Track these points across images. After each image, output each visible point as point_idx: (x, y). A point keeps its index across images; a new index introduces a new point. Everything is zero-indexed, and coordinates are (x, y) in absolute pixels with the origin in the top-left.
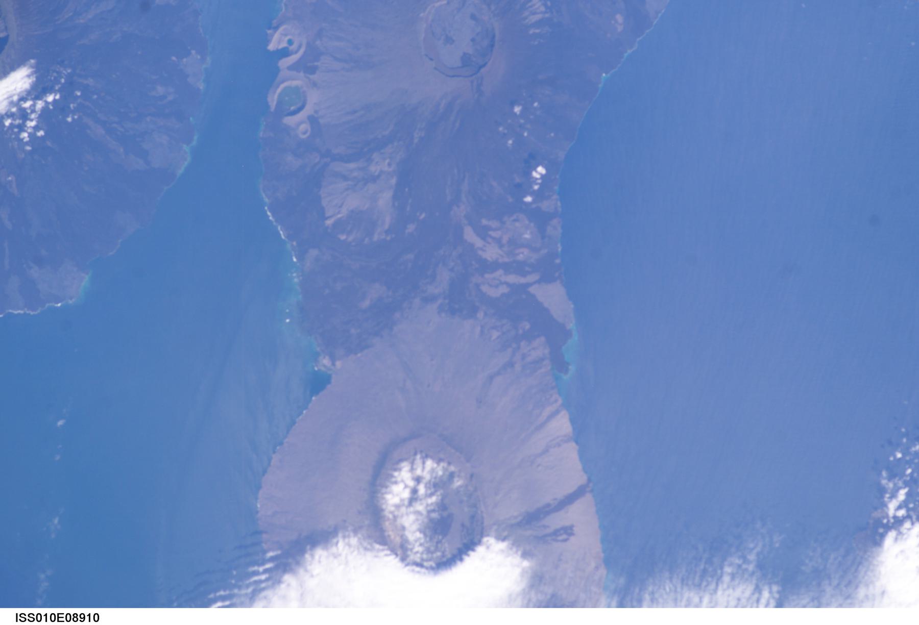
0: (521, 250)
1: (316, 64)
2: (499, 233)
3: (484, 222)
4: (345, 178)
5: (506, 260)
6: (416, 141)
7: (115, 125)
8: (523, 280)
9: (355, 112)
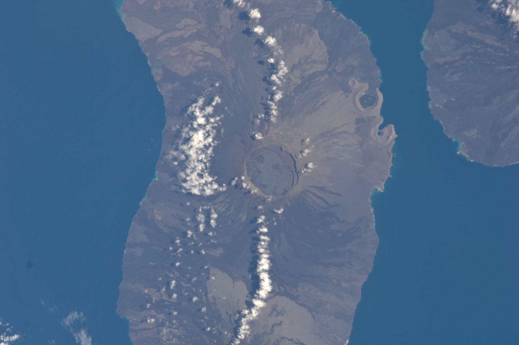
0: (176, 54)
1: (358, 126)
2: (196, 60)
3: (209, 63)
4: (314, 62)
5: (185, 44)
7: (479, 47)
8: (168, 35)
9: (323, 104)
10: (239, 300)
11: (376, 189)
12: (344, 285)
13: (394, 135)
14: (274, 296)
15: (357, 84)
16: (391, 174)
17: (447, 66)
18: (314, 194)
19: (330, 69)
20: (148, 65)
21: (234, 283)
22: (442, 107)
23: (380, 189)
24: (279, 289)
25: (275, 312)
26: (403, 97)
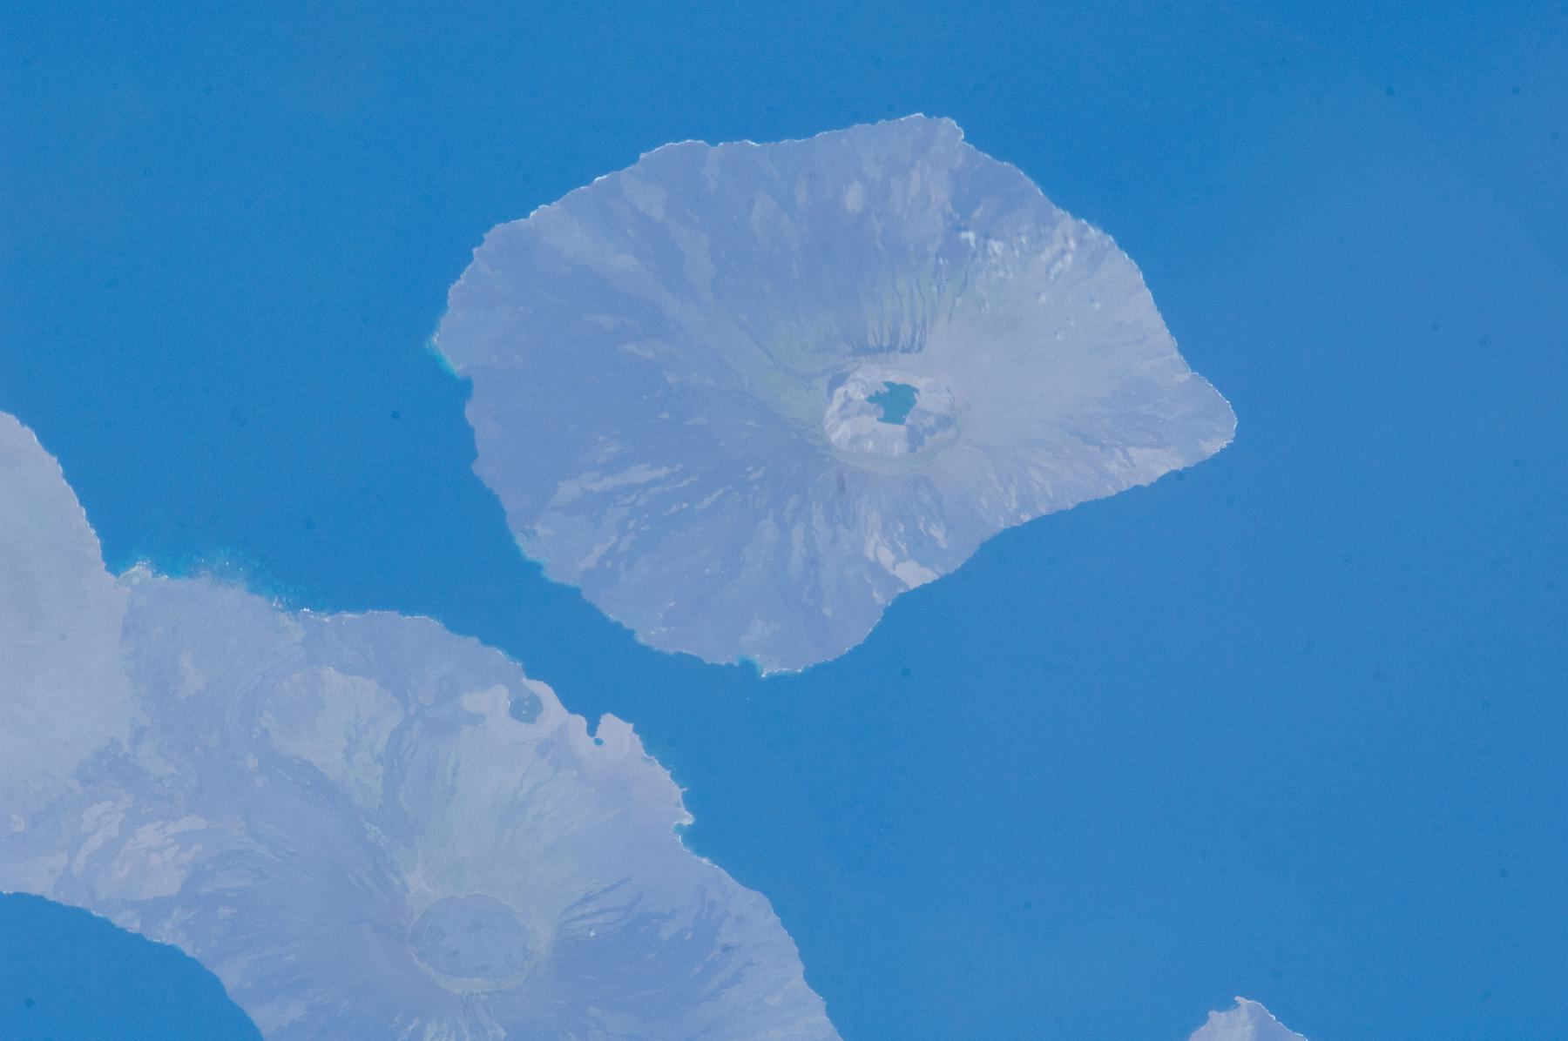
6: (367, 825)
11: (680, 826)
13: (628, 728)
17: (609, 564)
18: (583, 917)
19: (412, 711)
22: (664, 630)
23: (688, 820)
26: (583, 657)
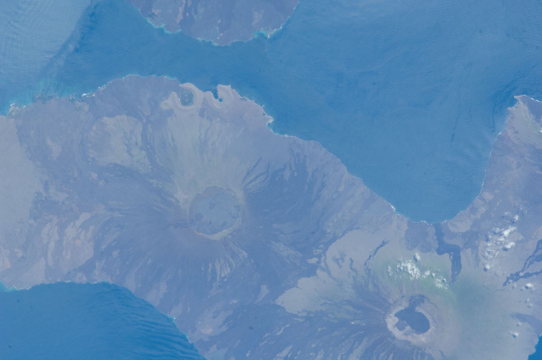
3: (92, 228)
6: (151, 181)
9: (173, 140)
10: (315, 289)
11: (269, 124)
12: (341, 189)
13: (228, 87)
14: (325, 256)
15: (169, 101)
16: (261, 105)
19: (145, 121)
20: (69, 283)
21: (298, 287)
22: (222, 34)
23: (271, 121)
24: (321, 248)
25: (340, 261)
